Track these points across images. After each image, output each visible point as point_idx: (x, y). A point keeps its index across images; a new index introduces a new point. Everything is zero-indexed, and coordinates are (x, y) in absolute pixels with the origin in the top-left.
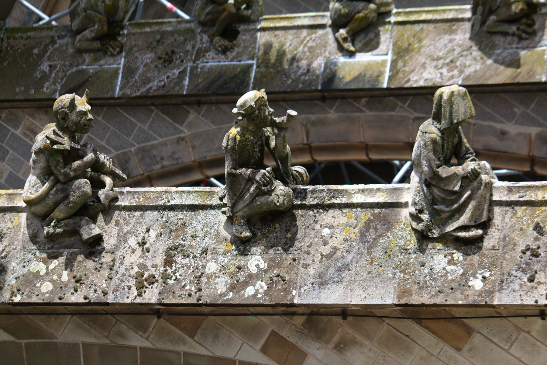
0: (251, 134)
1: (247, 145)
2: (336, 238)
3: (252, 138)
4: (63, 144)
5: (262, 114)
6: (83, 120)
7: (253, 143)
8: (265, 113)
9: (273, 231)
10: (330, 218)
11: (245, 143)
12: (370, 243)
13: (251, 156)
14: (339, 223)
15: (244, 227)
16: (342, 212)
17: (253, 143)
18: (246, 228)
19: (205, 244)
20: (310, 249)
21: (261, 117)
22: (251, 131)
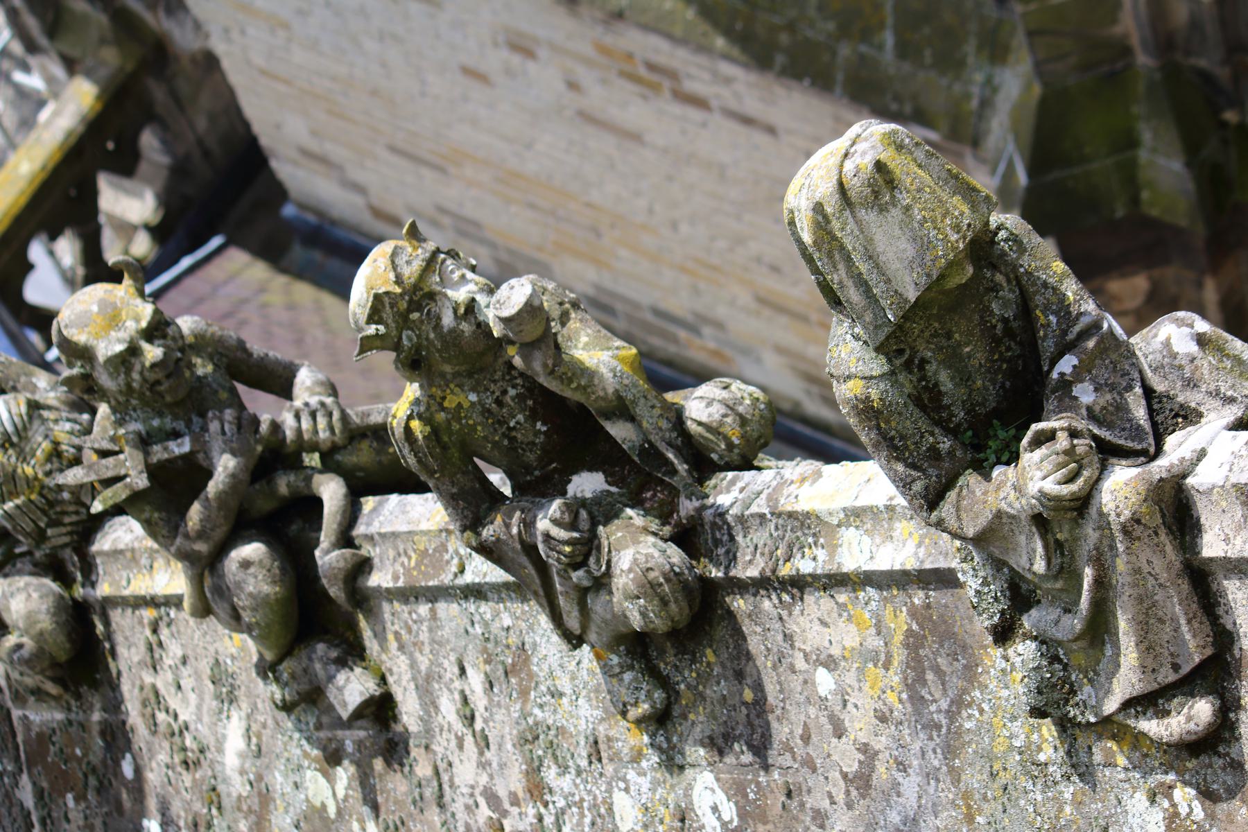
0: (460, 386)
1: (473, 428)
2: (856, 706)
3: (473, 397)
4: (125, 476)
5: (432, 336)
6: (136, 376)
7: (489, 411)
8: (438, 326)
9: (709, 675)
10: (817, 627)
11: (460, 424)
12: (944, 730)
13: (515, 449)
14: (844, 648)
15: (628, 676)
16: (837, 603)
17: (486, 412)
18: (635, 679)
19: (584, 720)
20: (810, 750)
21: (434, 346)
22: (456, 375)
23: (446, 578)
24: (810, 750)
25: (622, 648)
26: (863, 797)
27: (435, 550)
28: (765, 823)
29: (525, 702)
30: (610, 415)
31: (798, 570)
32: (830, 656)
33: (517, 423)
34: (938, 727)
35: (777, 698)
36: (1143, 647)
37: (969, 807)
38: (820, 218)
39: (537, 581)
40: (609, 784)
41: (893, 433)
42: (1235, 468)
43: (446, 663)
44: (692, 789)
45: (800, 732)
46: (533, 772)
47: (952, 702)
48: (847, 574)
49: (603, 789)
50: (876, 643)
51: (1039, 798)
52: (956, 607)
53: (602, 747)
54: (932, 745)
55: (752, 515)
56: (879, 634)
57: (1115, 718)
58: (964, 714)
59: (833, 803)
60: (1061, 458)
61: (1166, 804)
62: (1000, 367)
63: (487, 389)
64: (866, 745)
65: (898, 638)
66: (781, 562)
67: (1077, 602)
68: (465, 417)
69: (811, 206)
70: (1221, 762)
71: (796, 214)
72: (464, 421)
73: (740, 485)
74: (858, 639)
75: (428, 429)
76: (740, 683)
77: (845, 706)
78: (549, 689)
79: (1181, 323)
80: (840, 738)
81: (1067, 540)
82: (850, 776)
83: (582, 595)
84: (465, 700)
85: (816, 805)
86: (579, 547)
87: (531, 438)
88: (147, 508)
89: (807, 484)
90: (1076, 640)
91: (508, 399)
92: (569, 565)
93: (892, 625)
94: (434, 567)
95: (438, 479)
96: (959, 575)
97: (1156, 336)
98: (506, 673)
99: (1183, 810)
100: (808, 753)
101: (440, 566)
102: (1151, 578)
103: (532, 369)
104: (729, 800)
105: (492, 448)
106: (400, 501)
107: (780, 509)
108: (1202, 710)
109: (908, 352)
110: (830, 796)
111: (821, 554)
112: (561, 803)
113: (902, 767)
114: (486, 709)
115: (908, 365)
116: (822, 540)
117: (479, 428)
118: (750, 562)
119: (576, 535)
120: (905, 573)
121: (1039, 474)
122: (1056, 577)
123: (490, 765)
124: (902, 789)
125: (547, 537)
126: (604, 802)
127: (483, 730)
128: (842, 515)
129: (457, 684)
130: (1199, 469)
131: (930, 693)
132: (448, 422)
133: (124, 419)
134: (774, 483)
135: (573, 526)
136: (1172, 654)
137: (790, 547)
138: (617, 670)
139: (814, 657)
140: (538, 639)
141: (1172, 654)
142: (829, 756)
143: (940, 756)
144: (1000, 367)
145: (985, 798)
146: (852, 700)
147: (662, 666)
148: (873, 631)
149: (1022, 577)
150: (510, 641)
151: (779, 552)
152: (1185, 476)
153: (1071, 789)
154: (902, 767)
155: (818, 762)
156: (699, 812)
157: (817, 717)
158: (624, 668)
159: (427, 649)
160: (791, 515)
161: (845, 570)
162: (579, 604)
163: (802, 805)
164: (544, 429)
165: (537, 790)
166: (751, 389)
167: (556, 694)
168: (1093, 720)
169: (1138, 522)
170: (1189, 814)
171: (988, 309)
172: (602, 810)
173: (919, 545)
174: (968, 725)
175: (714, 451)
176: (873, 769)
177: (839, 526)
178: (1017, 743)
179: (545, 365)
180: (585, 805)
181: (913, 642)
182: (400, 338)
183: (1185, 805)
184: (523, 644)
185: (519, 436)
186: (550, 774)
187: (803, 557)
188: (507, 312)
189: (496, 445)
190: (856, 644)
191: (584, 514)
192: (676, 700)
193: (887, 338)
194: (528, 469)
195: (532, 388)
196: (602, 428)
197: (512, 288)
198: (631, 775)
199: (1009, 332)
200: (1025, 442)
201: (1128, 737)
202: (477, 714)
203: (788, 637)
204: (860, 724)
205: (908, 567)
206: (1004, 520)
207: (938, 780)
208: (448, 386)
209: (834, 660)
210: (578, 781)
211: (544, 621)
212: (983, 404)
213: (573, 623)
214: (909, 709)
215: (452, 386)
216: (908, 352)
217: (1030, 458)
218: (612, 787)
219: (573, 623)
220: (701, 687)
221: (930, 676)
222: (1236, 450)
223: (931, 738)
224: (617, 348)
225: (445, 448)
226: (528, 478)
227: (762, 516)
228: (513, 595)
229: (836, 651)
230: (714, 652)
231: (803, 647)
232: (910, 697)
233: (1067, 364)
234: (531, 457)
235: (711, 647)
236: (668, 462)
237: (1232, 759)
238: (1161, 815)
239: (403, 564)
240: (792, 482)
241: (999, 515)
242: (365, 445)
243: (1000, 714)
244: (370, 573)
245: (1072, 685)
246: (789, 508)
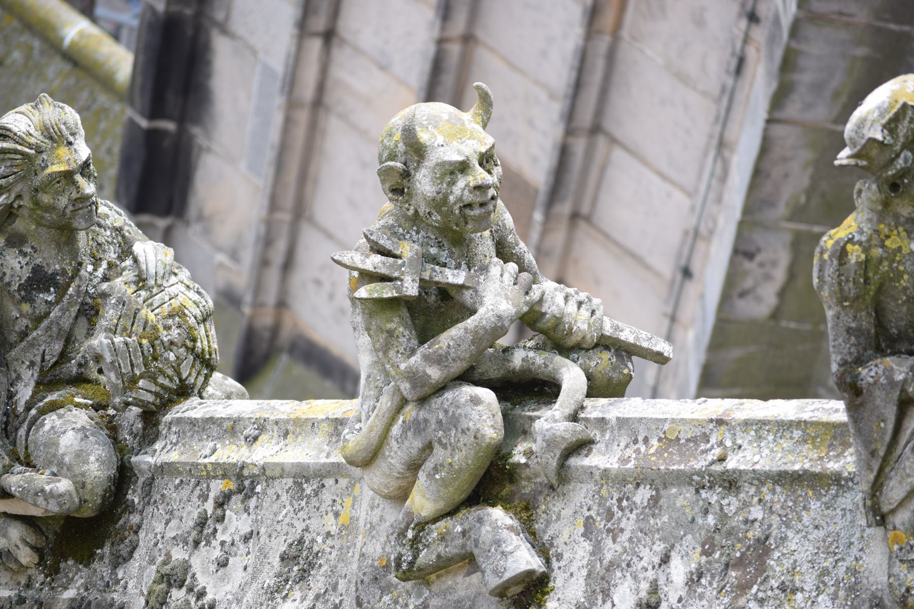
11: (890, 266)
68: (899, 262)
72: (895, 265)
75: (863, 257)
88: (396, 320)
117: (906, 277)
132: (880, 261)
133: (404, 236)
182: (898, 156)
208: (897, 228)
215: (901, 229)
225: (867, 280)
239: (638, 451)
242: (606, 355)
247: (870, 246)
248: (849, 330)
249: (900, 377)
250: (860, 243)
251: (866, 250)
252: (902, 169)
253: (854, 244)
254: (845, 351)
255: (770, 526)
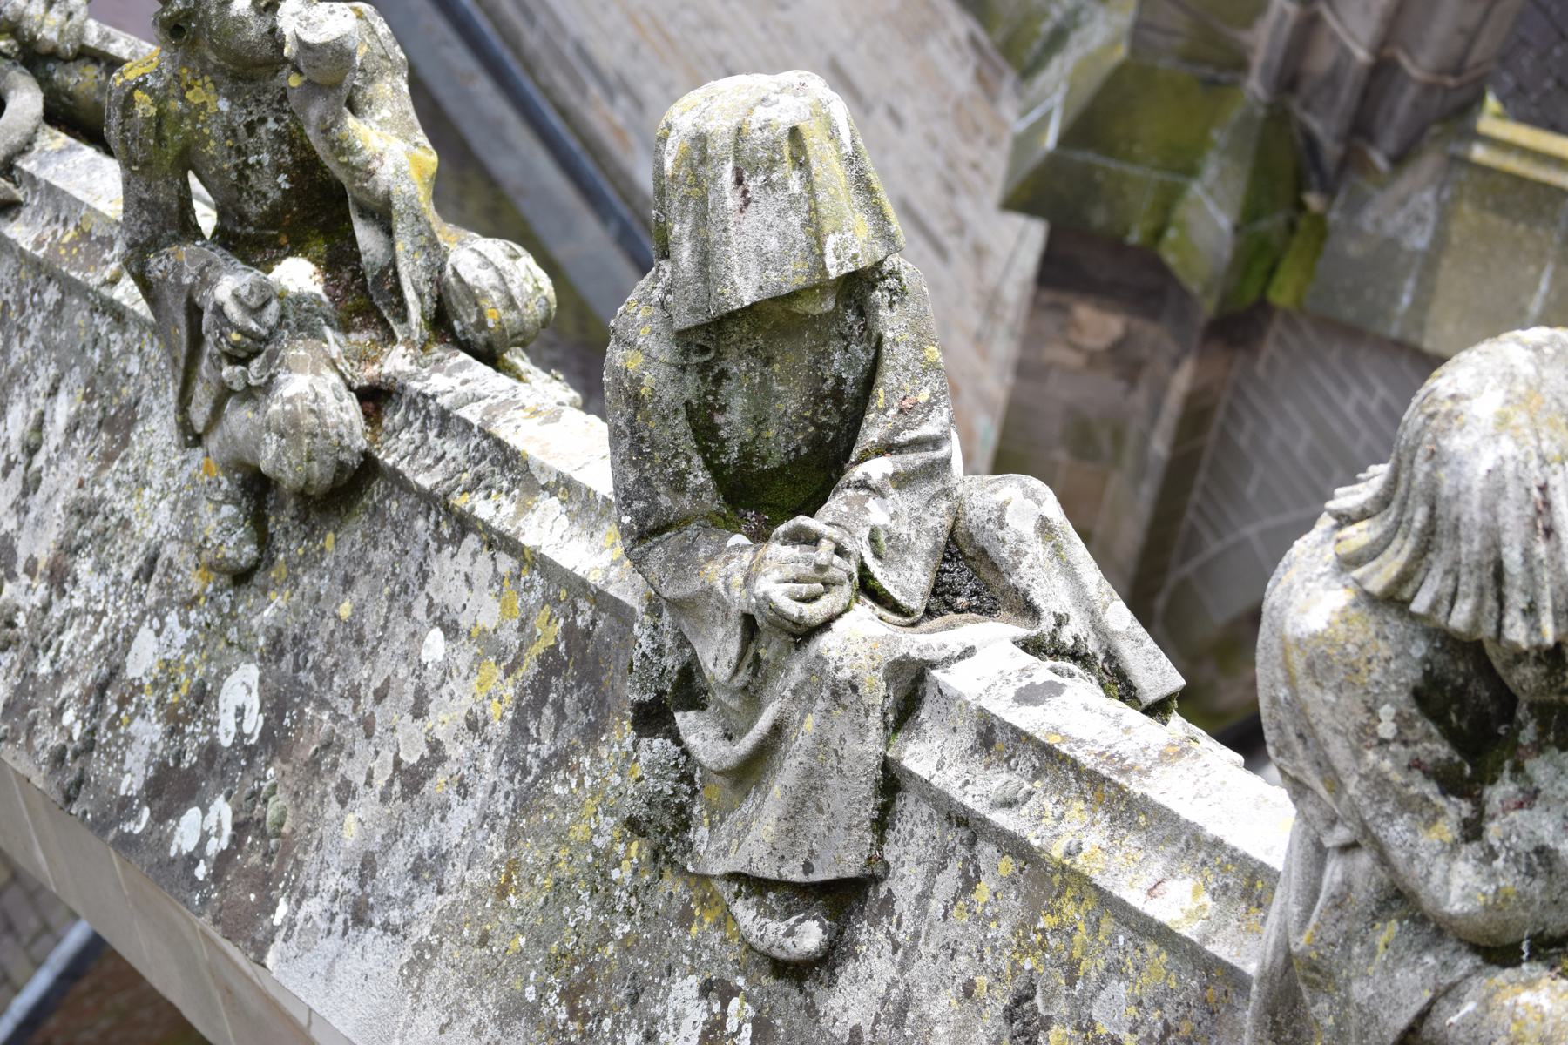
1: (205, 140)
2: (452, 696)
3: (224, 105)
5: (213, 12)
7: (234, 131)
10: (460, 581)
11: (193, 125)
12: (530, 779)
13: (240, 191)
15: (228, 510)
18: (234, 519)
19: (155, 528)
20: (378, 711)
22: (219, 69)
23: (94, 280)
24: (378, 711)
25: (237, 476)
26: (404, 797)
27: (98, 239)
28: (285, 761)
29: (100, 469)
30: (366, 213)
31: (473, 509)
32: (456, 622)
33: (259, 162)
34: (526, 771)
35: (374, 632)
36: (785, 825)
37: (509, 879)
38: (696, 155)
39: (184, 349)
40: (144, 614)
41: (646, 434)
42: (993, 691)
43: (41, 371)
44: (229, 674)
45: (378, 685)
46: (68, 549)
47: (555, 754)
48: (523, 547)
49: (134, 615)
50: (512, 639)
51: (589, 916)
52: (618, 655)
53: (159, 569)
54: (508, 786)
55: (459, 418)
56: (520, 629)
57: (714, 883)
58: (561, 776)
59: (369, 783)
60: (808, 570)
61: (716, 1007)
62: (805, 428)
63: (245, 106)
64: (439, 743)
65: (539, 649)
66: (460, 489)
67: (742, 733)
68: (204, 122)
69: (693, 134)
70: (799, 999)
71: (673, 133)
73: (465, 375)
74: (495, 624)
75: (153, 111)
76: (344, 592)
77: (438, 688)
78: (136, 470)
79: (1031, 495)
80: (416, 717)
81: (768, 662)
82: (403, 766)
83: (224, 394)
84: (39, 425)
85: (349, 776)
86: (249, 341)
87: (264, 188)
89: (538, 419)
90: (719, 773)
91: (262, 131)
92: (226, 354)
93: (539, 631)
94: (87, 258)
95: (134, 172)
96: (636, 626)
97: (995, 491)
98: (100, 424)
99: (731, 1026)
100: (372, 713)
101: (93, 262)
102: (834, 757)
103: (306, 116)
104: (261, 711)
105: (215, 175)
106: (93, 160)
107: (492, 429)
108: (810, 936)
109: (712, 354)
110: (370, 775)
111: (508, 508)
112: (78, 603)
113: (464, 790)
114: (57, 450)
115: (704, 368)
116: (517, 492)
117: (212, 143)
118: (429, 468)
119: (254, 326)
120: (584, 584)
121: (776, 575)
122: (734, 694)
123: (27, 513)
124: (449, 815)
125: (219, 310)
126: (126, 630)
127: (40, 470)
128: (553, 479)
129: (41, 401)
130: (956, 667)
131: (538, 729)
134: (502, 397)
135: (256, 312)
136: (811, 852)
137: (479, 478)
138: (219, 497)
139: (438, 614)
140: (155, 407)
141: (811, 852)
142: (393, 730)
143: (510, 805)
144: (805, 428)
145: (531, 881)
146: (451, 685)
147: (272, 519)
148: (516, 623)
149: (700, 669)
150: (124, 390)
151: (465, 476)
152: (933, 665)
153: (627, 929)
154: (464, 790)
155: (379, 729)
156: (222, 705)
157: (405, 680)
158: (228, 498)
159: (29, 342)
160: (499, 443)
161: (523, 540)
162: (215, 402)
163: (335, 765)
164: (287, 186)
165: (59, 577)
166: (541, 274)
167: (141, 482)
168: (690, 868)
169: (855, 689)
170: (734, 1035)
171: (826, 355)
172: (119, 639)
173: (614, 563)
174: (558, 790)
175: (459, 318)
176: (430, 775)
177: (544, 488)
178: (599, 843)
179: (322, 119)
180: (105, 620)
181: (551, 664)
183: (736, 1021)
184: (137, 403)
185: (253, 178)
186: (83, 567)
187: (488, 496)
188: (310, 37)
189: (220, 172)
190: (490, 626)
191: (274, 307)
192: (267, 567)
193: (698, 327)
194: (243, 219)
195: (292, 139)
196: (351, 223)
197: (332, 12)
198: (172, 619)
199: (837, 394)
200: (782, 528)
201: (718, 910)
202: (44, 448)
203: (424, 575)
204: (445, 718)
205: (591, 580)
206: (712, 601)
207: (492, 828)
209: (457, 631)
210: (111, 590)
211: (171, 396)
212: (763, 459)
213: (199, 416)
214: (507, 731)
215: (207, 79)
216: (712, 354)
217: (777, 551)
218: (143, 618)
219: (199, 416)
220: (300, 570)
221: (547, 711)
222: (1006, 672)
223: (511, 779)
224: (416, 144)
226: (238, 230)
227: (468, 426)
228: (156, 342)
229: (464, 623)
230: (336, 540)
231: (432, 594)
232: (514, 721)
233: (878, 468)
234: (253, 209)
235: (336, 532)
236: (402, 303)
237: (813, 1004)
238: (705, 1016)
239: (54, 233)
240: (523, 407)
241: (709, 592)
243: (598, 799)
244: (12, 220)
245: (689, 817)
246: (502, 435)
247: (167, 97)
248: (140, 202)
249: (187, 280)
250: (151, 92)
251: (159, 102)
252: (181, 12)
253: (145, 91)
254: (135, 229)
255: (142, 387)
